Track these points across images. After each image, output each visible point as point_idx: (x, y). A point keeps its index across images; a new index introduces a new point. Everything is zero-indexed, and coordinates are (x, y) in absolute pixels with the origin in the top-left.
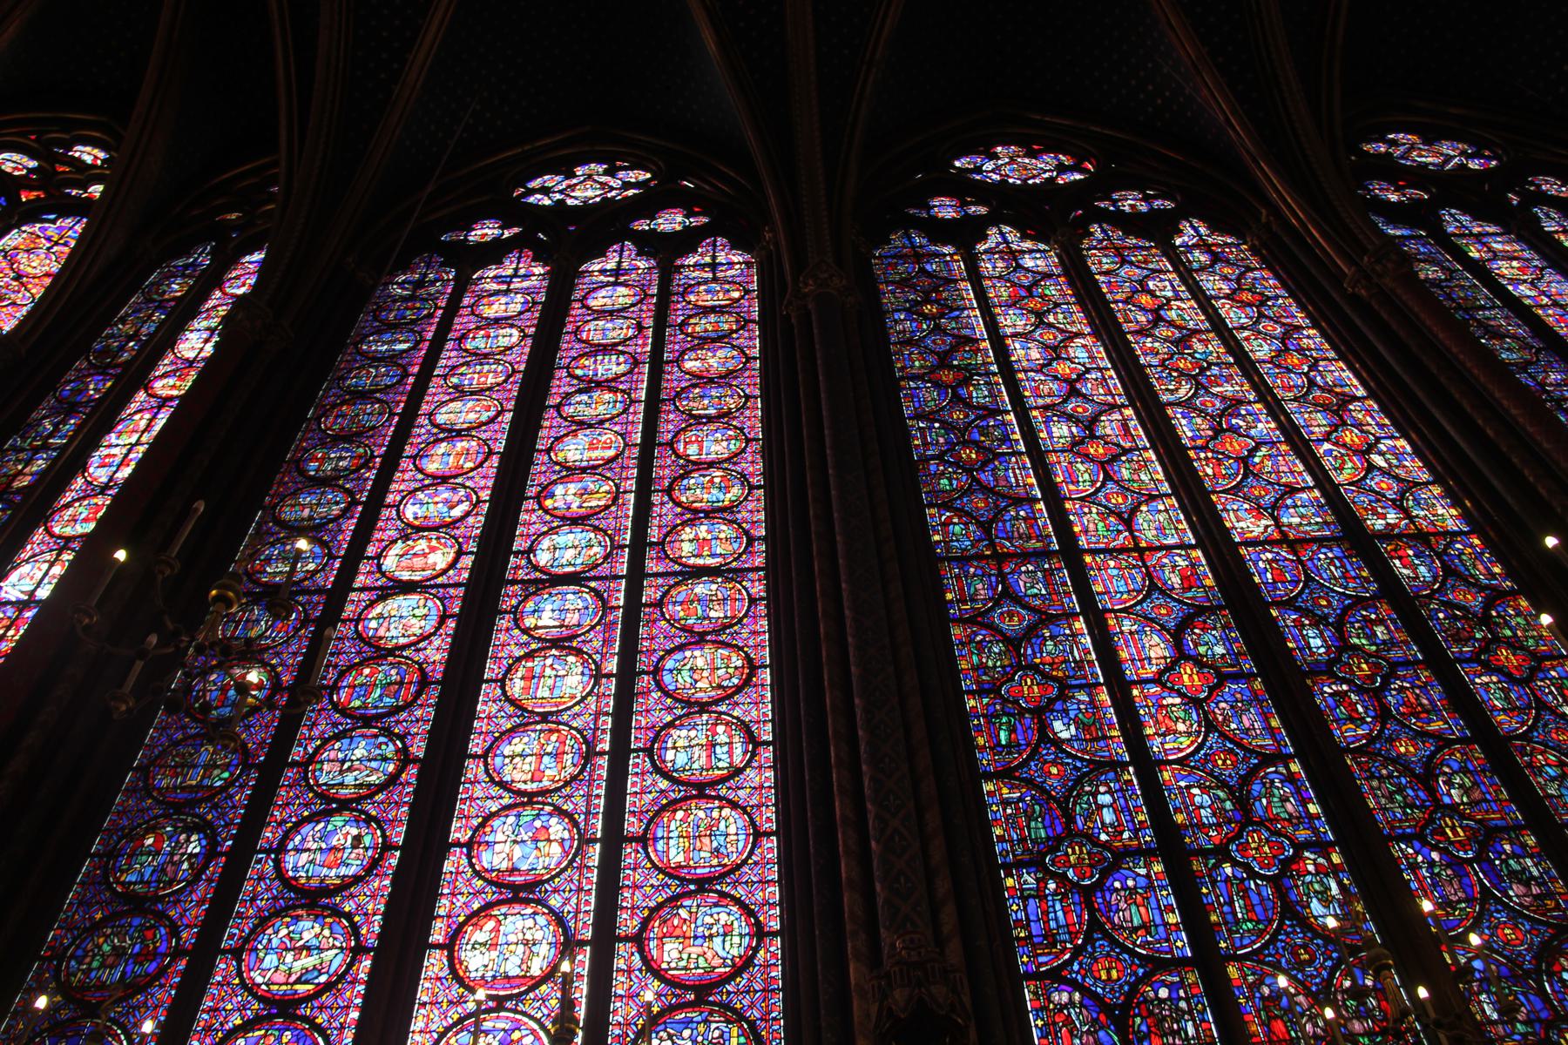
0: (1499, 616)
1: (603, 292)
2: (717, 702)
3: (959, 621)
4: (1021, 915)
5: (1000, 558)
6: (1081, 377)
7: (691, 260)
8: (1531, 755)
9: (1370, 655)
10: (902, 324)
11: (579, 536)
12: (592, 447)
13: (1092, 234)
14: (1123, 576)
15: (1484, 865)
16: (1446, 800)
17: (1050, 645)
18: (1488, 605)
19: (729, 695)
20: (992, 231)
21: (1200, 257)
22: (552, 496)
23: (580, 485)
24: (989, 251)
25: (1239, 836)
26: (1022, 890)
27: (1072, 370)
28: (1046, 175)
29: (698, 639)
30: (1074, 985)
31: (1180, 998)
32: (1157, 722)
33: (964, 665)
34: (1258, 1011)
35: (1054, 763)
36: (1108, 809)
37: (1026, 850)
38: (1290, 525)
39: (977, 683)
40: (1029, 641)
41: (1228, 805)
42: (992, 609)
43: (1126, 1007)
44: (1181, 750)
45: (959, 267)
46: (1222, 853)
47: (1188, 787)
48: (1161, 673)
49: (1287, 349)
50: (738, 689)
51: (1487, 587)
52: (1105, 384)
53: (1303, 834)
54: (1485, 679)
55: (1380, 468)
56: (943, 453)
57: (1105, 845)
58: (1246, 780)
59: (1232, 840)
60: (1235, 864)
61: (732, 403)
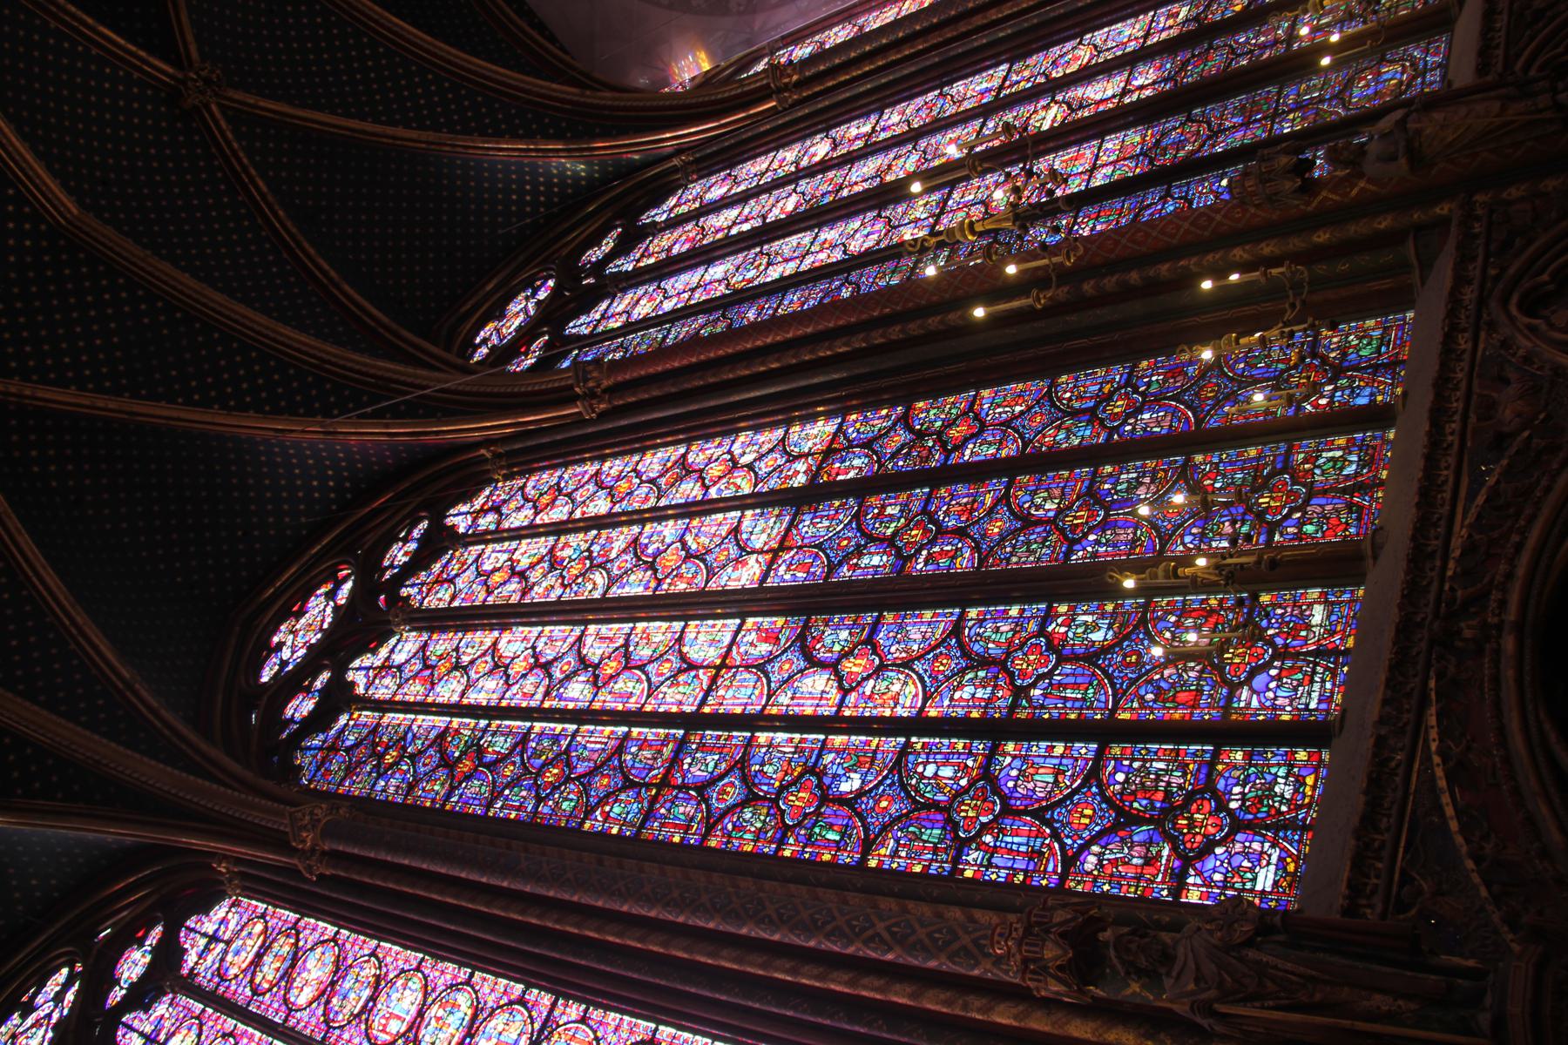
4: (1003, 873)
5: (665, 782)
6: (536, 656)
10: (390, 787)
13: (409, 596)
14: (738, 687)
16: (1051, 514)
17: (769, 769)
18: (910, 429)
20: (350, 676)
25: (1011, 675)
26: (981, 865)
27: (525, 659)
28: (329, 610)
30: (1085, 848)
31: (1130, 766)
34: (1164, 708)
35: (877, 802)
36: (941, 769)
39: (771, 842)
40: (755, 785)
41: (982, 674)
42: (709, 806)
43: (1120, 812)
44: (916, 695)
45: (367, 717)
46: (1020, 693)
47: (952, 699)
48: (840, 687)
49: (611, 487)
51: (894, 424)
52: (556, 639)
53: (1032, 626)
54: (968, 452)
57: (971, 783)
59: (1012, 683)
60: (1033, 685)
61: (369, 971)
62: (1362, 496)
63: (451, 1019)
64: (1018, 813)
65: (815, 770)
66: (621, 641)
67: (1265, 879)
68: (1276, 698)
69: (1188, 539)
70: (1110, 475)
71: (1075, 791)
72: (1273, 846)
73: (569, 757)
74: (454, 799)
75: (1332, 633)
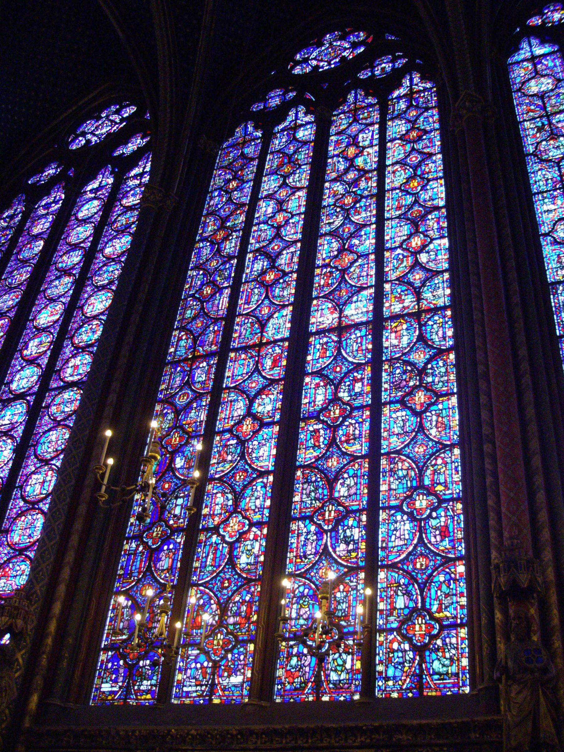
1: (86, 207)
2: (52, 458)
7: (133, 173)
8: (396, 463)
9: (344, 403)
11: (31, 370)
18: (429, 361)
21: (402, 105)
22: (27, 348)
25: (227, 519)
32: (220, 456)
37: (139, 529)
38: (347, 317)
41: (230, 503)
46: (215, 530)
47: (217, 493)
53: (256, 518)
54: (399, 414)
56: (197, 291)
58: (245, 487)
60: (219, 535)
62: (312, 687)
63: (90, 334)
66: (287, 270)
68: (191, 669)
69: (301, 589)
70: (360, 520)
74: (201, 245)
75: (223, 690)
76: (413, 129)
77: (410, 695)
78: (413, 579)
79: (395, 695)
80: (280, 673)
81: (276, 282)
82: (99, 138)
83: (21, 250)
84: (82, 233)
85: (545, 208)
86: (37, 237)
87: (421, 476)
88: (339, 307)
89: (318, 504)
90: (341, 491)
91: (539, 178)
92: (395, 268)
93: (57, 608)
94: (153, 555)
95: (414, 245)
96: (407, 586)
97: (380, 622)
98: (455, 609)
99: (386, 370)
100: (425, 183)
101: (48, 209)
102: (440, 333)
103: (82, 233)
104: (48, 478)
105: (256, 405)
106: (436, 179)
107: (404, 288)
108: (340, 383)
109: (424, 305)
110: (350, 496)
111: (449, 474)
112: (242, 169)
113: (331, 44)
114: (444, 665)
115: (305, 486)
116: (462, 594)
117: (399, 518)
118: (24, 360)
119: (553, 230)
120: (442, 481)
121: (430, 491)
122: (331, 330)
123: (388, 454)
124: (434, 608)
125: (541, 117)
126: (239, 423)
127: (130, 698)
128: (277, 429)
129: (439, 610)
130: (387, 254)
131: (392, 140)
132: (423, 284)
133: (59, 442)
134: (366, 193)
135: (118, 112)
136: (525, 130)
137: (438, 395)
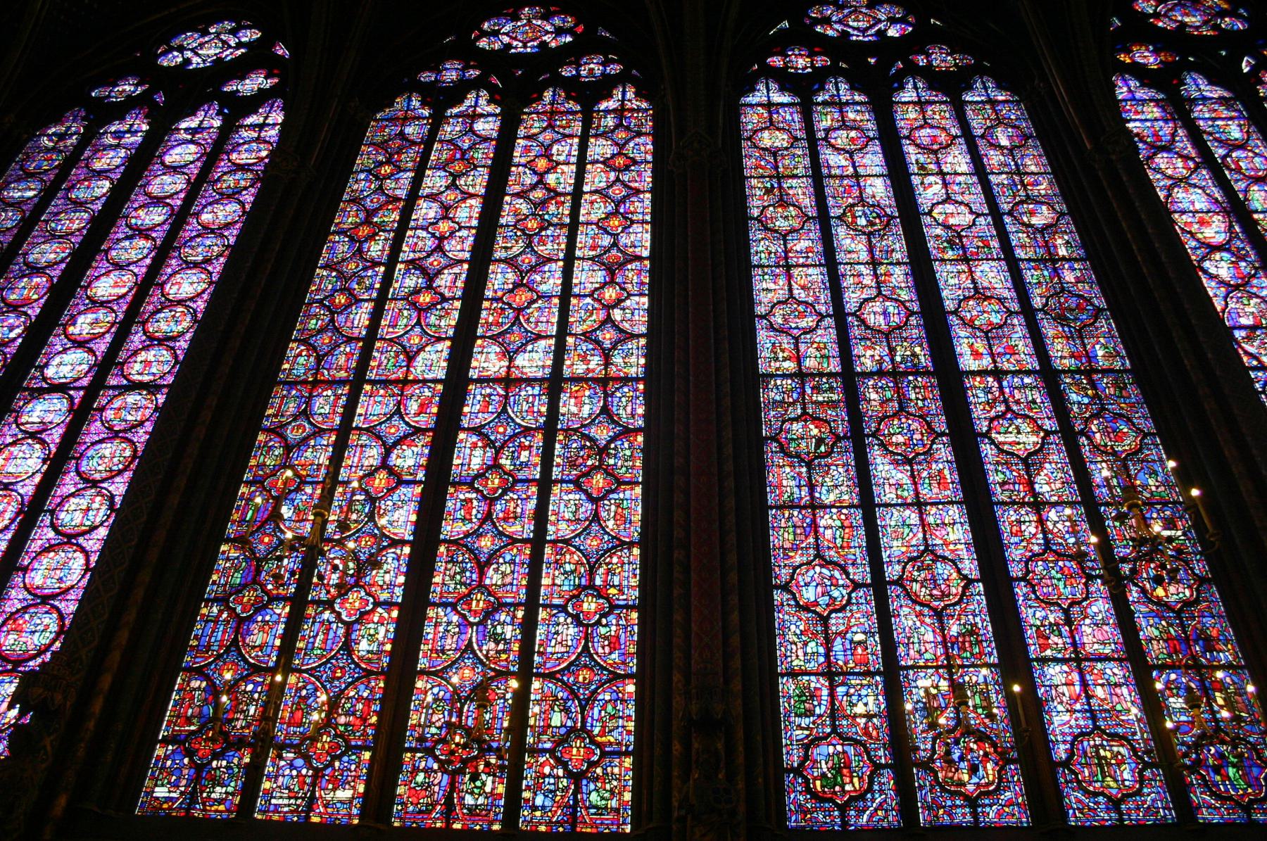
0: (614, 449)
1: (178, 150)
2: (103, 481)
3: (268, 431)
7: (249, 121)
9: (505, 473)
12: (116, 285)
15: (481, 628)
17: (308, 454)
18: (613, 439)
19: (112, 475)
21: (610, 121)
22: (74, 324)
23: (94, 316)
24: (457, 116)
29: (113, 435)
33: (253, 462)
35: (268, 535)
42: (290, 423)
46: (329, 605)
50: (120, 472)
53: (384, 596)
54: (571, 496)
55: (613, 322)
56: (326, 297)
60: (333, 611)
64: (237, 631)
65: (303, 482)
66: (447, 294)
67: (161, 792)
69: (436, 690)
70: (514, 617)
71: (246, 661)
72: (182, 793)
73: (350, 306)
75: (326, 806)
76: (620, 154)
77: (561, 829)
78: (574, 694)
79: (543, 828)
80: (400, 790)
81: (432, 306)
82: (204, 61)
83: (73, 187)
84: (168, 185)
85: (765, 286)
86: (101, 174)
87: (591, 573)
88: (509, 355)
89: (464, 590)
90: (492, 578)
91: (761, 249)
92: (582, 320)
93: (106, 681)
94: (241, 624)
95: (607, 296)
96: (566, 701)
97: (530, 740)
98: (621, 734)
99: (560, 442)
100: (628, 223)
101: (120, 138)
102: (629, 409)
103: (168, 185)
104: (96, 506)
105: (394, 456)
106: (643, 222)
107: (591, 346)
108: (502, 447)
109: (613, 371)
110: (504, 585)
111: (625, 577)
112: (399, 153)
113: (529, 21)
114: (602, 798)
115: (449, 566)
116: (629, 718)
117: (562, 620)
118: (69, 340)
119: (770, 313)
120: (616, 583)
121: (600, 593)
122: (497, 380)
123: (554, 542)
124: (596, 731)
125: (771, 177)
126: (371, 474)
127: (195, 808)
128: (418, 490)
129: (602, 734)
130: (574, 301)
131: (594, 162)
132: (614, 347)
133: (115, 460)
134: (555, 220)
135: (234, 32)
136: (752, 188)
137: (620, 482)
